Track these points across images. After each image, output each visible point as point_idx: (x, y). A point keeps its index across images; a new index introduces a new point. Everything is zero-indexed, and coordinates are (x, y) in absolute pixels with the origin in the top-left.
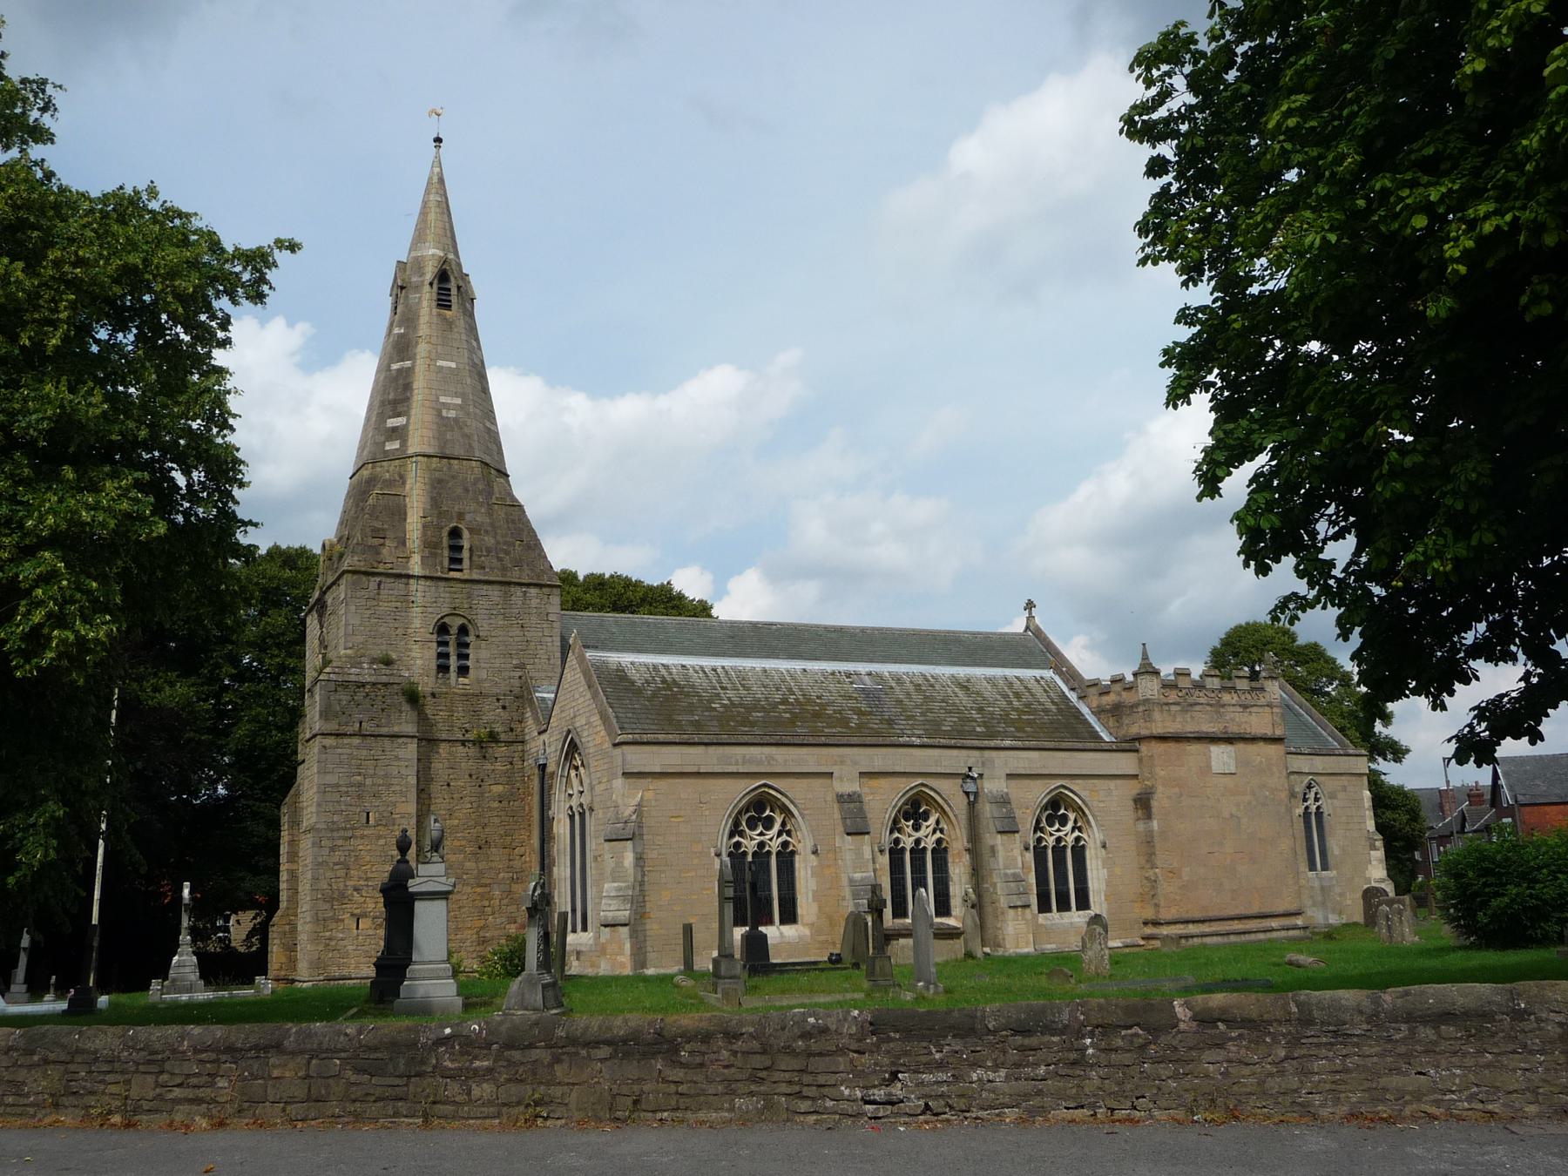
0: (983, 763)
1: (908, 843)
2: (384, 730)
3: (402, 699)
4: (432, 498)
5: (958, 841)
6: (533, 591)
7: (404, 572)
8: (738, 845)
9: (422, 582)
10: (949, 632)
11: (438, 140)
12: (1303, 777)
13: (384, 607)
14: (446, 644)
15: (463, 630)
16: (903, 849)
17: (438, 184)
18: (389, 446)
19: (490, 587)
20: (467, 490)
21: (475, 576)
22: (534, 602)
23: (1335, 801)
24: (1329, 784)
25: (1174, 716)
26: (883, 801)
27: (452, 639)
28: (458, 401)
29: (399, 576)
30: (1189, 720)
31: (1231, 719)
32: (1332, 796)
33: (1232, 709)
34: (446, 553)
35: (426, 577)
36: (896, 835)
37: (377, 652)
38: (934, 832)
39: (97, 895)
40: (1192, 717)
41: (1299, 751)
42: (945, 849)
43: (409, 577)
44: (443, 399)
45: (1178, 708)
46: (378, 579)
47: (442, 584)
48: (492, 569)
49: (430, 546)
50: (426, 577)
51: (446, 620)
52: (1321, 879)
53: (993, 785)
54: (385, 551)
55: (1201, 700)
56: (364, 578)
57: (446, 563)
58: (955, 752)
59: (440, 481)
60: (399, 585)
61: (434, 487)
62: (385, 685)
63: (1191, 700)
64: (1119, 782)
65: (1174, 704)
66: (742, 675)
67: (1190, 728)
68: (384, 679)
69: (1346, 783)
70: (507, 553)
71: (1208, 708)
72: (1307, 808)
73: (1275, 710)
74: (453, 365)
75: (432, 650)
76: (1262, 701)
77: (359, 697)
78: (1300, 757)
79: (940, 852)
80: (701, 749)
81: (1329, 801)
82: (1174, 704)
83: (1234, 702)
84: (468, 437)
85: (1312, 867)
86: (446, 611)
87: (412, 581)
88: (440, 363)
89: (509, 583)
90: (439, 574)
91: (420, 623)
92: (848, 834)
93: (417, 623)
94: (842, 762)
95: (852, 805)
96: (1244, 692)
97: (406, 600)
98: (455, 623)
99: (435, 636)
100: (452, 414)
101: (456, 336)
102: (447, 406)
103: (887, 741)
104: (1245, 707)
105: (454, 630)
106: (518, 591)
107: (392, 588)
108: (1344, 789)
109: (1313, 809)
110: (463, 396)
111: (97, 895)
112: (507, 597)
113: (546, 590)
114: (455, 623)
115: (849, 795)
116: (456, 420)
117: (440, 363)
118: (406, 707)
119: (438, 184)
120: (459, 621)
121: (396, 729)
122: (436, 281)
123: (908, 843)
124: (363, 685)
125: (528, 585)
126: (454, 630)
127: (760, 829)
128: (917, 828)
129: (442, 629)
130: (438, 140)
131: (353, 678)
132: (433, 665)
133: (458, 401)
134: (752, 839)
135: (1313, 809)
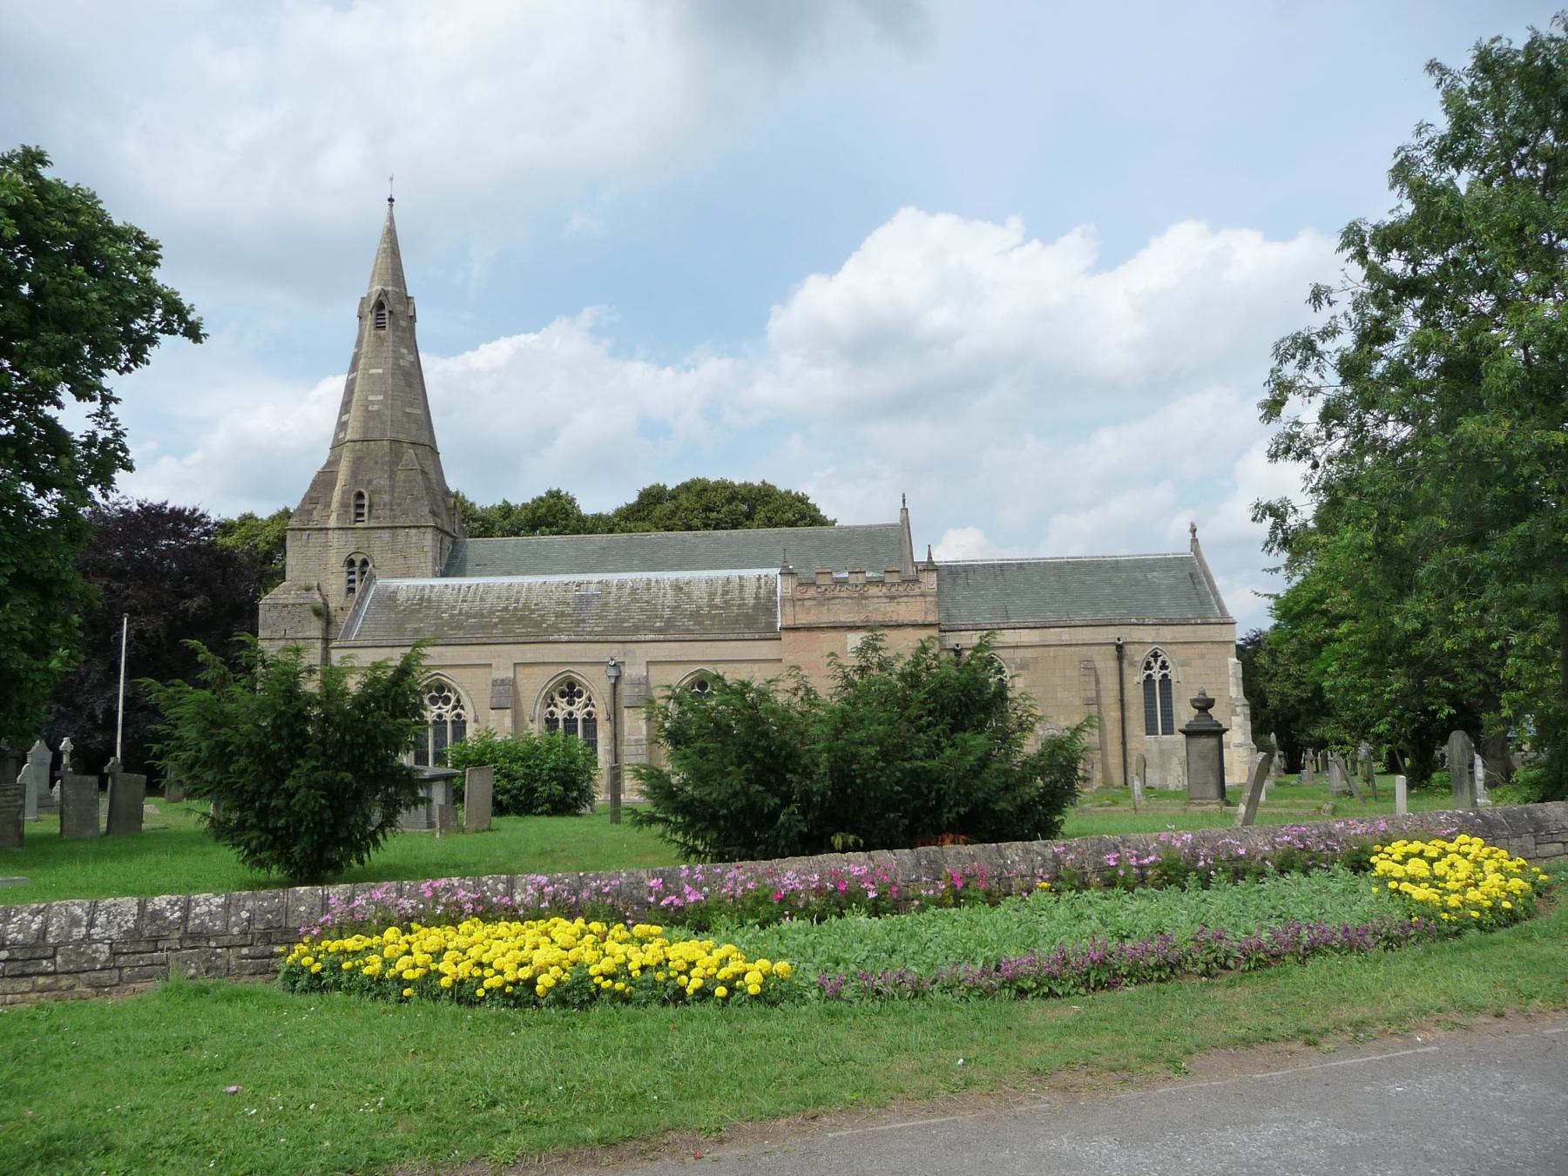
0: (625, 654)
1: (560, 715)
2: (300, 635)
3: (311, 613)
4: (352, 472)
5: (601, 714)
6: (413, 531)
7: (323, 526)
8: (552, 713)
9: (336, 532)
10: (871, 527)
11: (391, 200)
12: (1146, 646)
13: (311, 552)
14: (353, 573)
15: (365, 563)
16: (576, 720)
17: (391, 233)
18: (119, 453)
19: (383, 531)
20: (377, 463)
21: (372, 525)
22: (414, 539)
23: (1188, 669)
24: (1182, 652)
25: (809, 609)
26: (533, 685)
27: (356, 569)
28: (381, 397)
29: (321, 529)
30: (825, 612)
31: (875, 609)
32: (1184, 664)
33: (876, 600)
34: (352, 510)
35: (339, 529)
36: (552, 708)
37: (302, 583)
38: (587, 706)
39: (119, 740)
40: (828, 609)
41: (1141, 621)
42: (595, 720)
43: (327, 529)
44: (370, 398)
45: (814, 602)
46: (308, 532)
47: (350, 531)
48: (385, 518)
49: (344, 505)
50: (339, 529)
51: (353, 557)
52: (1160, 743)
53: (632, 671)
54: (315, 513)
55: (843, 594)
56: (299, 533)
57: (352, 517)
58: (598, 646)
59: (359, 458)
60: (322, 535)
61: (354, 463)
62: (301, 605)
63: (828, 594)
64: (763, 665)
65: (810, 599)
66: (488, 589)
67: (825, 617)
68: (301, 601)
69: (1204, 651)
70: (399, 505)
71: (850, 601)
72: (1149, 676)
73: (929, 599)
74: (381, 371)
75: (343, 579)
76: (917, 591)
77: (284, 613)
78: (1141, 627)
79: (590, 722)
80: (389, 649)
81: (1179, 669)
82: (810, 599)
83: (880, 594)
84: (384, 423)
85: (1151, 729)
86: (352, 550)
87: (330, 532)
88: (372, 371)
89: (396, 527)
90: (348, 526)
91: (335, 560)
92: (492, 709)
93: (333, 560)
94: (499, 657)
95: (501, 688)
96: (893, 585)
97: (326, 546)
98: (358, 559)
99: (345, 569)
100: (376, 408)
101: (385, 349)
102: (372, 402)
103: (539, 639)
104: (892, 598)
105: (358, 564)
106: (402, 532)
107: (317, 538)
108: (1202, 656)
109: (1157, 677)
110: (384, 393)
111: (119, 740)
112: (394, 537)
113: (423, 530)
114: (358, 559)
115: (502, 680)
116: (378, 411)
117: (372, 371)
118: (314, 618)
119: (391, 233)
120: (361, 557)
121: (307, 634)
122: (374, 311)
123: (560, 715)
124: (287, 606)
125: (409, 527)
126: (358, 564)
127: (440, 704)
128: (571, 703)
129: (351, 563)
130: (391, 200)
131: (281, 601)
132: (344, 589)
133: (381, 397)
134: (432, 712)
135: (1157, 677)
